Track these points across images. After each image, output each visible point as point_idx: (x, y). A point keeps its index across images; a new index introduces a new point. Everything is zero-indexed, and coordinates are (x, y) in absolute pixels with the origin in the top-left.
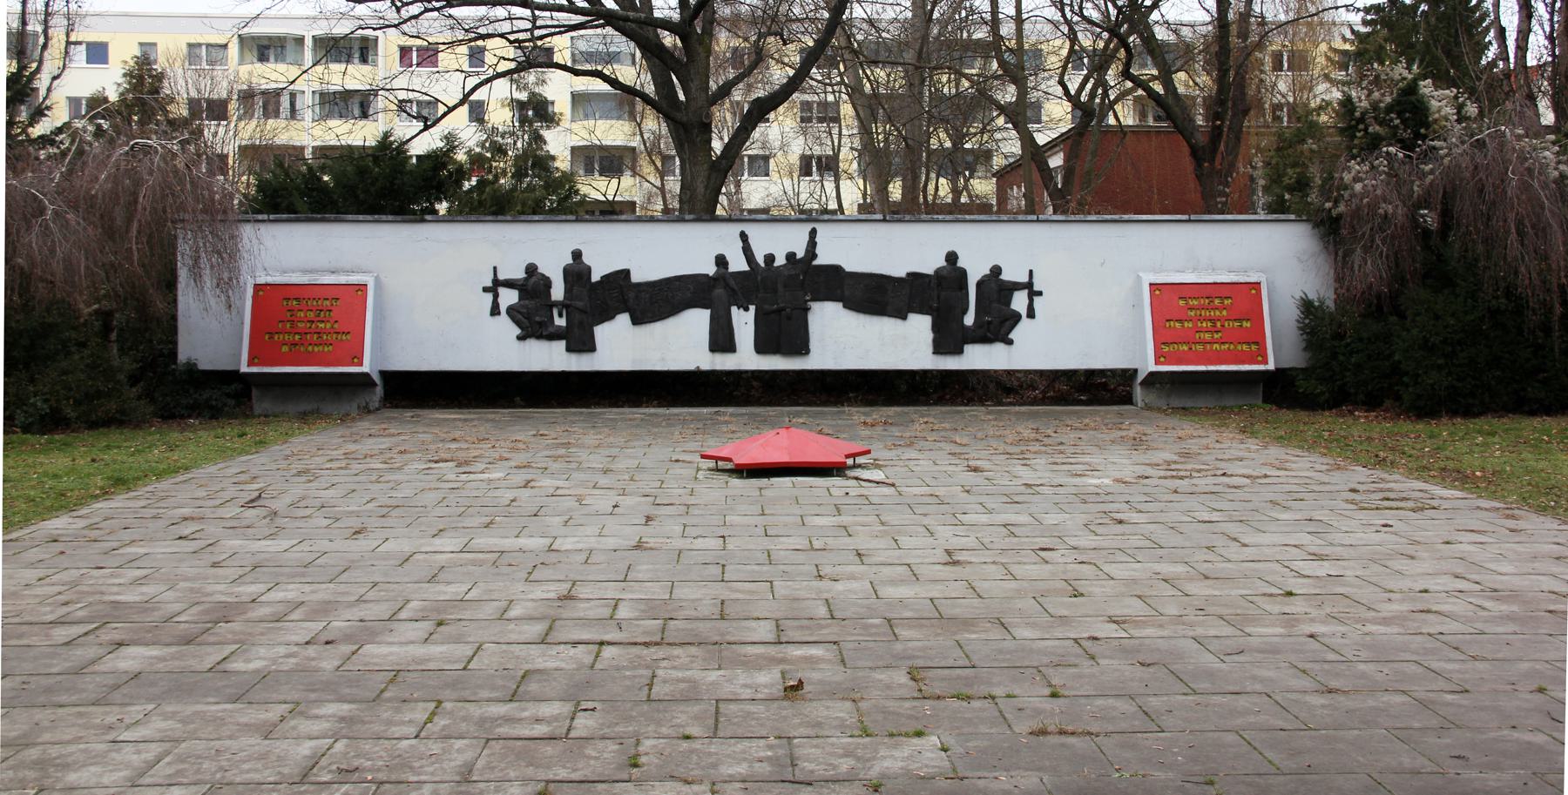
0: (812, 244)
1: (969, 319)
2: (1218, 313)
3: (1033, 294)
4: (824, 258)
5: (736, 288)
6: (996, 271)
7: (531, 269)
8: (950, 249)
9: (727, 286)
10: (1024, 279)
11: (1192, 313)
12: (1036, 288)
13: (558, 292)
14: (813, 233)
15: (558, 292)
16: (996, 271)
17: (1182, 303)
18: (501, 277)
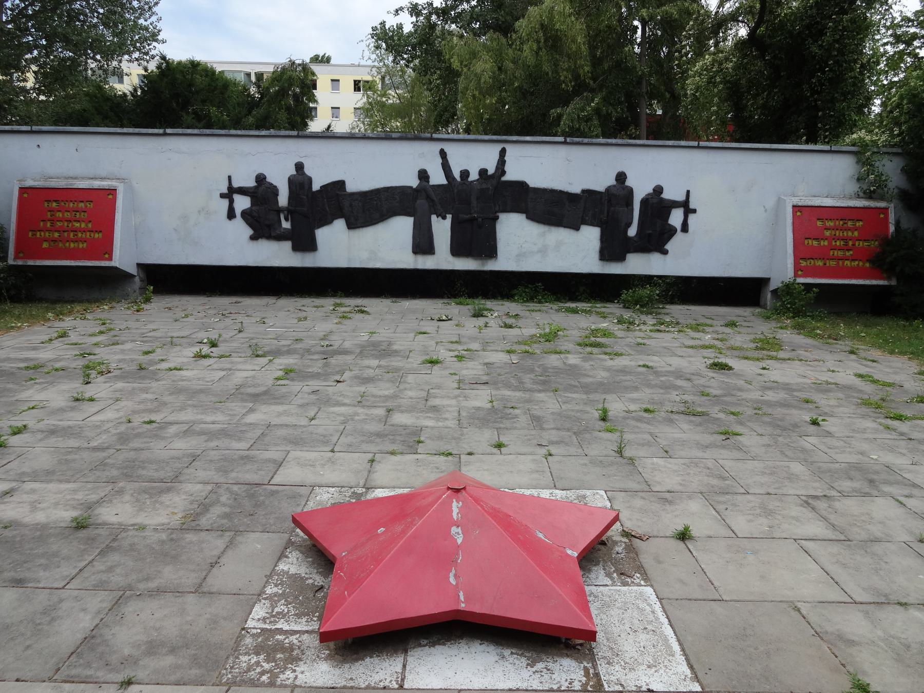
0: (502, 162)
1: (632, 232)
2: (850, 234)
3: (689, 211)
4: (512, 174)
5: (435, 198)
6: (658, 190)
7: (261, 179)
8: (620, 170)
9: (428, 197)
10: (681, 197)
11: (827, 233)
12: (692, 206)
13: (283, 199)
14: (503, 152)
15: (283, 199)
16: (658, 190)
17: (819, 223)
18: (236, 185)
